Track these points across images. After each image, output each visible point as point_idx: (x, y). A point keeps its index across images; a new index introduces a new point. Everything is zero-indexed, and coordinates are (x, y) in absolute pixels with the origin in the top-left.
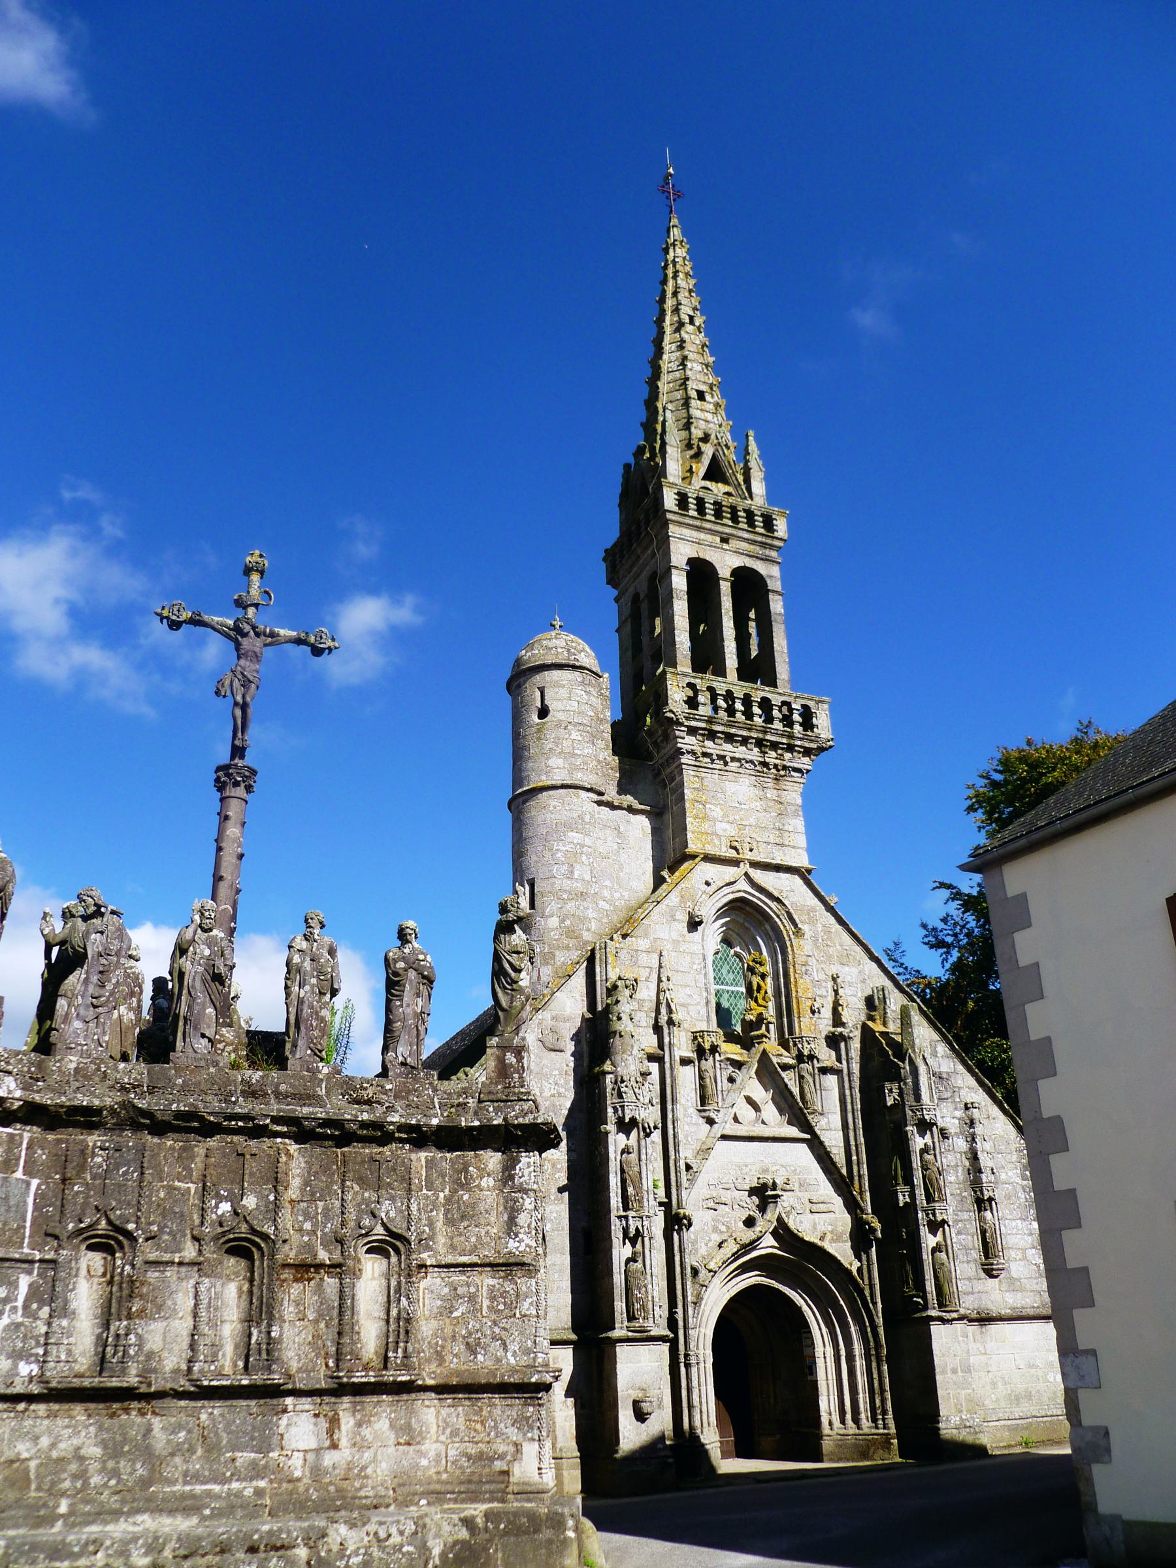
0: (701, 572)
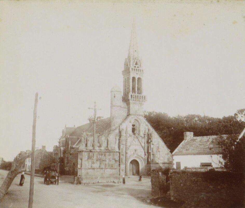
0: (134, 78)
